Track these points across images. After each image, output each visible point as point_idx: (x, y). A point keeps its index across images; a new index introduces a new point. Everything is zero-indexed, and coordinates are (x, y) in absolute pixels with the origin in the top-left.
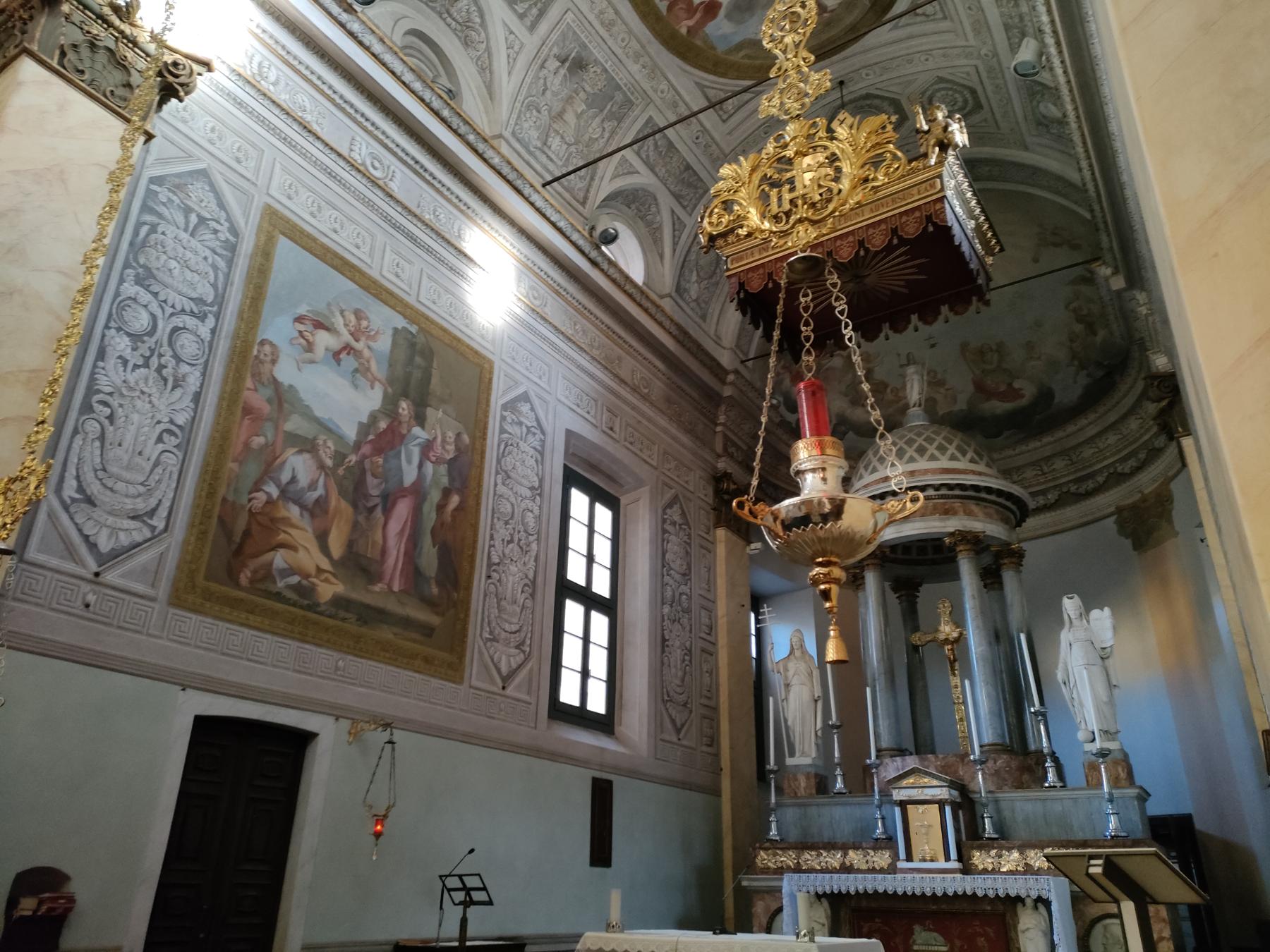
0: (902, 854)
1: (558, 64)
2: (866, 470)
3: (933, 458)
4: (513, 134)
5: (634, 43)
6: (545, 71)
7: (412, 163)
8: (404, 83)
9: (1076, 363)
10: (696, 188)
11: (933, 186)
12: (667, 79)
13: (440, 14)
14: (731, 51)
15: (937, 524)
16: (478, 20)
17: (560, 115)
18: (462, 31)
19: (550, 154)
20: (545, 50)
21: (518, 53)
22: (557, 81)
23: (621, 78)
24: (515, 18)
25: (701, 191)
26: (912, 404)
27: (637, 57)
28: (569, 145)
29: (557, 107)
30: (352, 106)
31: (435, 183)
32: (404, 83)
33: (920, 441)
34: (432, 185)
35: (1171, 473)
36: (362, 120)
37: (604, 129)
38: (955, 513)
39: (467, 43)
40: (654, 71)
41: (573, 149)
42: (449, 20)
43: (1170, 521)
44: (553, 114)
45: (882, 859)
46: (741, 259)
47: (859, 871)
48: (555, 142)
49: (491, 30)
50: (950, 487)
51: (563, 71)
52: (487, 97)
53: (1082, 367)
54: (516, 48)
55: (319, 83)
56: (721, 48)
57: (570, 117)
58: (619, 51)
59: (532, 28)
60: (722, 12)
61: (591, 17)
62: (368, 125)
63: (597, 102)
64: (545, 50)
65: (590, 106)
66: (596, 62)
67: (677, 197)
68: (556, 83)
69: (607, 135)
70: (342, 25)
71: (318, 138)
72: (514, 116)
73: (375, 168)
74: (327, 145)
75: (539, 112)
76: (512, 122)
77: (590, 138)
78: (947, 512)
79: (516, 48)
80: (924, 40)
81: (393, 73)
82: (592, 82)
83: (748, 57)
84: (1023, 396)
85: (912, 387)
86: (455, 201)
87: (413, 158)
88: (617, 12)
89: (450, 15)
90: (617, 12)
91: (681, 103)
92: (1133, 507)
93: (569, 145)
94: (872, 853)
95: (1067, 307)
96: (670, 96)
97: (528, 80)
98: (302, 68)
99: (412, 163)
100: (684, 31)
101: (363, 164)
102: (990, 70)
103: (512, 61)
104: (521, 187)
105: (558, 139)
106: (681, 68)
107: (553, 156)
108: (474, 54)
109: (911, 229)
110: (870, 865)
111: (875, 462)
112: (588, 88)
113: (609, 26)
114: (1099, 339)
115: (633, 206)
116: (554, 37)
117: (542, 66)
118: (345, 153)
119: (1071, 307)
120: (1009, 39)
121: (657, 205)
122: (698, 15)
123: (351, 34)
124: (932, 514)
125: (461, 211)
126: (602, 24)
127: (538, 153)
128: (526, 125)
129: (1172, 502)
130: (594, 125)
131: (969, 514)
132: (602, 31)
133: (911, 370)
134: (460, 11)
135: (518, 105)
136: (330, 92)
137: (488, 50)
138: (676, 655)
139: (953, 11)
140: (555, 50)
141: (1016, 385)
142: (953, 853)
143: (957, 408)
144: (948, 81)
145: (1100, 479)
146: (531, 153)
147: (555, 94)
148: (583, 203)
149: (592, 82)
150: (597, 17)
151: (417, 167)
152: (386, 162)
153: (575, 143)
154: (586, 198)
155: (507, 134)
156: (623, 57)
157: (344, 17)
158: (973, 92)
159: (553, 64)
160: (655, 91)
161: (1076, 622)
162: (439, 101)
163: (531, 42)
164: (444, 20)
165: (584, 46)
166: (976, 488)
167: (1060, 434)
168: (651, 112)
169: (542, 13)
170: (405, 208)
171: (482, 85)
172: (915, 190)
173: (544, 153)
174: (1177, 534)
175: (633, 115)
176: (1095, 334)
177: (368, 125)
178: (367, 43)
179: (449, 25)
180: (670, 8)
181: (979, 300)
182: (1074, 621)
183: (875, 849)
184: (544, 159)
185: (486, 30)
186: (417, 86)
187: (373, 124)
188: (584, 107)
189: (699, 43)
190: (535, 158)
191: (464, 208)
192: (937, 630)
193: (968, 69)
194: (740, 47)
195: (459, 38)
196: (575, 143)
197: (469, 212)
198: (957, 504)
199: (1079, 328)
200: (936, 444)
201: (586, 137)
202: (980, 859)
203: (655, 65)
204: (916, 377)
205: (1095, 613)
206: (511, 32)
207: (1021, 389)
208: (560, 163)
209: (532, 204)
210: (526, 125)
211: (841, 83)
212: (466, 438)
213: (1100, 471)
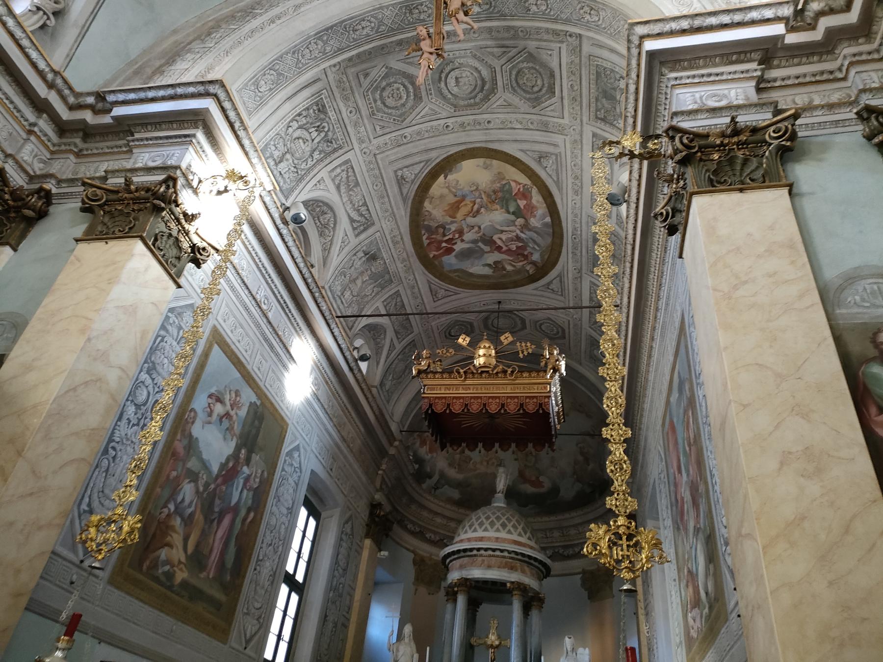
1: (363, 255)
3: (509, 532)
4: (330, 287)
5: (405, 255)
6: (355, 257)
7: (282, 302)
8: (296, 262)
10: (408, 330)
11: (545, 388)
12: (414, 275)
13: (314, 218)
14: (450, 271)
15: (506, 574)
16: (332, 225)
17: (354, 281)
18: (321, 228)
19: (343, 300)
20: (360, 247)
21: (345, 246)
22: (359, 263)
23: (392, 268)
24: (351, 229)
25: (409, 332)
26: (498, 491)
27: (404, 260)
28: (354, 296)
29: (354, 276)
30: (266, 269)
31: (289, 314)
32: (296, 262)
34: (288, 316)
36: (267, 277)
37: (373, 291)
38: (516, 570)
39: (321, 234)
40: (409, 269)
41: (354, 299)
42: (317, 221)
43: (611, 588)
44: (351, 279)
46: (433, 389)
48: (347, 294)
49: (337, 232)
50: (516, 553)
51: (364, 259)
52: (322, 264)
54: (346, 243)
55: (254, 255)
56: (447, 268)
57: (359, 282)
58: (395, 256)
59: (357, 236)
60: (454, 253)
61: (388, 237)
62: (269, 280)
63: (374, 277)
64: (360, 247)
65: (370, 278)
66: (383, 258)
67: (396, 332)
68: (358, 264)
69: (373, 294)
70: (278, 229)
71: (248, 288)
72: (333, 278)
73: (265, 304)
74: (250, 292)
75: (345, 277)
76: (331, 281)
77: (365, 295)
78: (512, 568)
79: (346, 243)
80: (547, 300)
81: (293, 257)
82: (377, 267)
83: (458, 276)
84: (543, 487)
86: (296, 325)
87: (284, 300)
88: (402, 238)
89: (319, 219)
90: (402, 238)
91: (416, 288)
93: (354, 296)
95: (577, 445)
96: (412, 282)
97: (346, 260)
98: (249, 247)
99: (282, 302)
100: (431, 256)
101: (260, 301)
102: (575, 325)
103: (342, 249)
104: (331, 324)
105: (349, 292)
106: (424, 273)
107: (344, 301)
108: (323, 241)
109: (531, 408)
111: (476, 526)
112: (373, 269)
113: (395, 243)
114: (590, 467)
115: (372, 332)
116: (366, 242)
117: (355, 255)
118: (254, 293)
119: (580, 445)
120: (590, 317)
121: (385, 335)
122: (441, 251)
123: (281, 235)
124: (504, 567)
125: (296, 331)
126: (392, 241)
127: (338, 299)
128: (337, 283)
130: (369, 288)
131: (523, 572)
132: (391, 245)
133: (501, 470)
134: (325, 218)
135: (337, 272)
136: (258, 261)
137: (331, 241)
138: (330, 625)
139: (567, 294)
140: (364, 248)
141: (541, 479)
144: (552, 321)
146: (334, 298)
147: (356, 269)
148: (350, 329)
149: (377, 267)
150: (391, 238)
151: (284, 305)
152: (270, 301)
153: (357, 296)
154: (353, 326)
155: (326, 287)
156: (396, 260)
157: (281, 226)
158: (563, 330)
159: (361, 254)
160: (406, 279)
161: (569, 653)
162: (309, 274)
163: (354, 241)
164: (315, 221)
165: (379, 249)
166: (530, 557)
167: (560, 517)
168: (400, 288)
169: (365, 229)
170: (274, 329)
171: (321, 257)
172: (536, 387)
173: (340, 299)
174: (614, 596)
175: (390, 287)
177: (269, 280)
178: (287, 240)
179: (316, 224)
180: (429, 244)
181: (549, 447)
182: (569, 653)
184: (339, 302)
185: (334, 231)
186: (302, 265)
187: (272, 280)
188: (367, 278)
189: (436, 263)
190: (336, 301)
191: (298, 330)
192: (487, 637)
193: (564, 320)
194: (456, 271)
195: (319, 231)
196: (357, 296)
197: (300, 332)
198: (518, 564)
199: (580, 458)
200: (506, 517)
201: (363, 293)
203: (411, 267)
204: (504, 476)
205: (580, 650)
206: (346, 235)
207: (542, 482)
208: (346, 305)
209: (333, 333)
210: (337, 283)
211: (500, 302)
212: (266, 474)
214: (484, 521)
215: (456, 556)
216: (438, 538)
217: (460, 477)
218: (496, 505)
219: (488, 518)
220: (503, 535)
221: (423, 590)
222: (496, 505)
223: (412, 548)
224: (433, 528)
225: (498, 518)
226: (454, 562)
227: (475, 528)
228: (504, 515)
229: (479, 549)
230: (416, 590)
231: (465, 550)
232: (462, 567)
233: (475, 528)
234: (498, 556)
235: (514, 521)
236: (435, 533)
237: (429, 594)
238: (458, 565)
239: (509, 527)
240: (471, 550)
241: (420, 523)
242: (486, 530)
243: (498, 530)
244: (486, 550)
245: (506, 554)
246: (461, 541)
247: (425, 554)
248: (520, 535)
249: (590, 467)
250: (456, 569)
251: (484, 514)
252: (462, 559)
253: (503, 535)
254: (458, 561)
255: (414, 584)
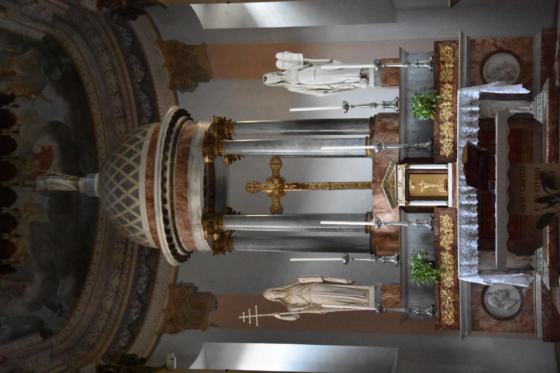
0: (443, 203)
2: (135, 218)
3: (138, 161)
9: (33, 96)
26: (74, 188)
33: (112, 178)
35: (155, 38)
43: (193, 48)
45: (445, 220)
47: (455, 240)
50: (166, 149)
53: (39, 92)
84: (50, 148)
85: (58, 184)
92: (174, 75)
94: (442, 229)
110: (451, 231)
114: (19, 71)
124: (186, 165)
129: (178, 42)
141: (37, 150)
142: (443, 167)
143: (46, 205)
145: (143, 97)
161: (283, 78)
174: (204, 44)
176: (14, 73)
181: (7, 104)
183: (439, 226)
202: (446, 150)
205: (279, 65)
207: (43, 148)
213: (136, 96)
214: (123, 197)
215: (174, 237)
216: (137, 303)
217: (38, 278)
218: (96, 189)
219: (119, 193)
220: (142, 169)
221: (212, 317)
222: (96, 189)
223: (155, 337)
224: (123, 311)
225: (119, 178)
226: (181, 239)
227: (134, 210)
228: (113, 171)
229: (164, 201)
230: (212, 325)
231: (166, 222)
232: (188, 227)
233: (134, 210)
234: (171, 174)
235: (121, 156)
236: (130, 307)
237: (216, 307)
238: (186, 232)
239: (130, 161)
240: (165, 212)
241: (116, 328)
242: (136, 194)
243: (136, 177)
244: (164, 191)
245: (168, 163)
246: (153, 231)
247: (162, 319)
248: (140, 147)
249: (19, 71)
250: (191, 235)
251: (109, 205)
252: (178, 227)
253: (142, 169)
254: (179, 234)
255: (204, 330)
